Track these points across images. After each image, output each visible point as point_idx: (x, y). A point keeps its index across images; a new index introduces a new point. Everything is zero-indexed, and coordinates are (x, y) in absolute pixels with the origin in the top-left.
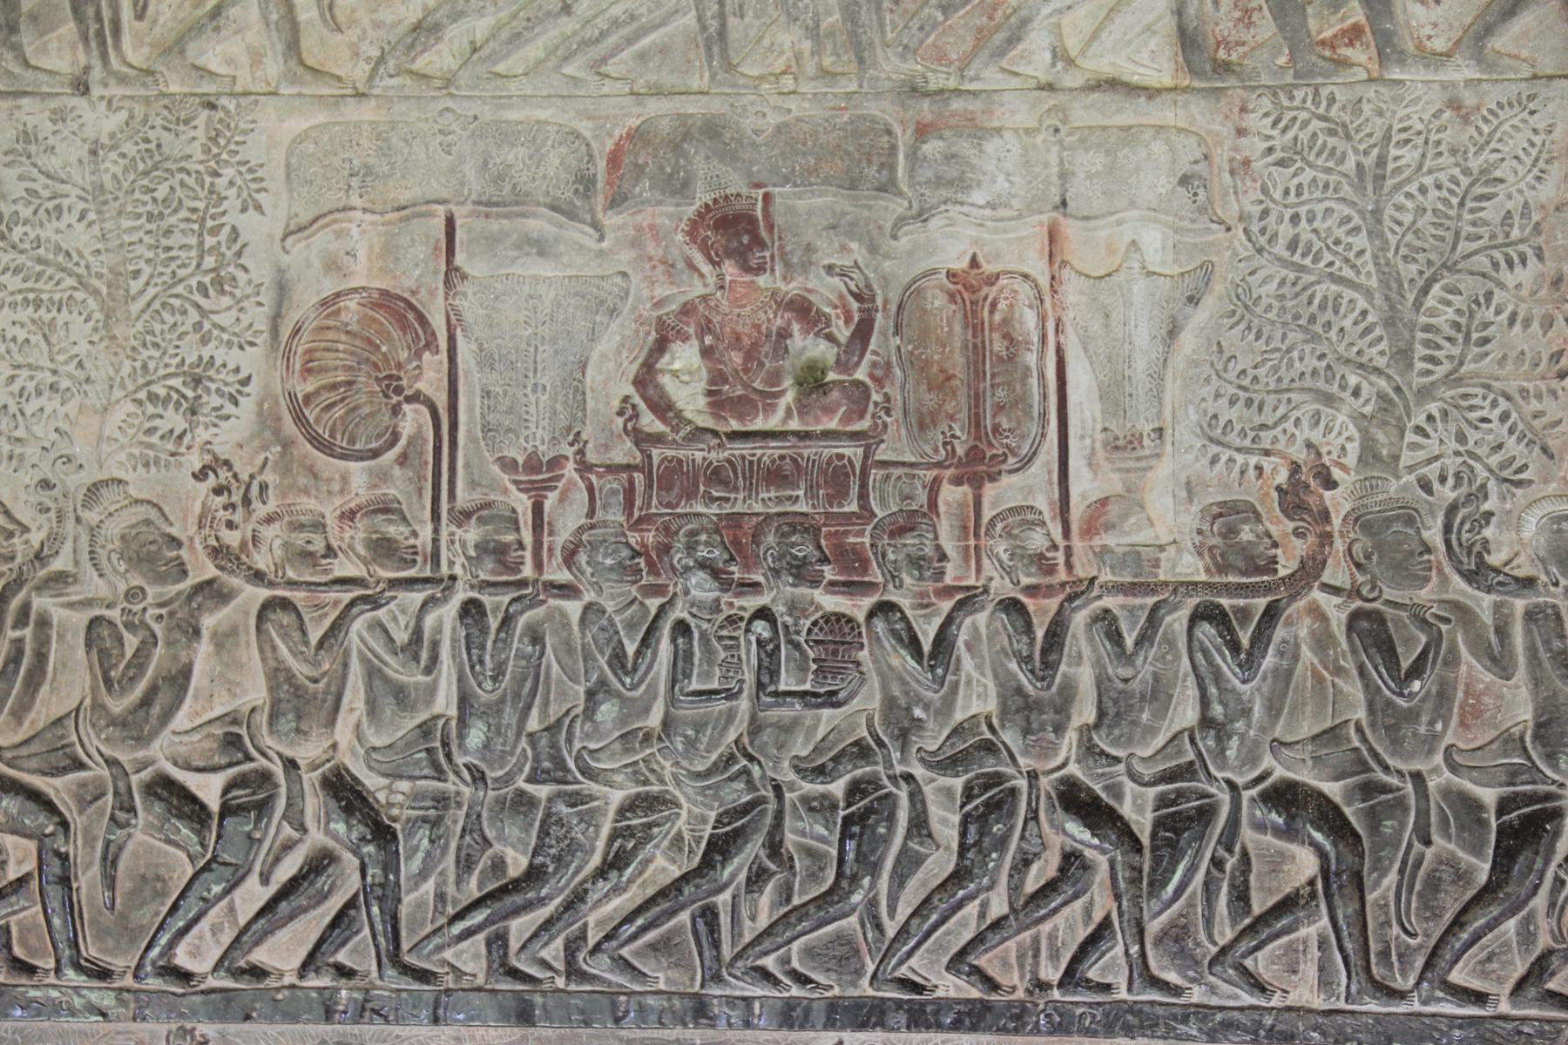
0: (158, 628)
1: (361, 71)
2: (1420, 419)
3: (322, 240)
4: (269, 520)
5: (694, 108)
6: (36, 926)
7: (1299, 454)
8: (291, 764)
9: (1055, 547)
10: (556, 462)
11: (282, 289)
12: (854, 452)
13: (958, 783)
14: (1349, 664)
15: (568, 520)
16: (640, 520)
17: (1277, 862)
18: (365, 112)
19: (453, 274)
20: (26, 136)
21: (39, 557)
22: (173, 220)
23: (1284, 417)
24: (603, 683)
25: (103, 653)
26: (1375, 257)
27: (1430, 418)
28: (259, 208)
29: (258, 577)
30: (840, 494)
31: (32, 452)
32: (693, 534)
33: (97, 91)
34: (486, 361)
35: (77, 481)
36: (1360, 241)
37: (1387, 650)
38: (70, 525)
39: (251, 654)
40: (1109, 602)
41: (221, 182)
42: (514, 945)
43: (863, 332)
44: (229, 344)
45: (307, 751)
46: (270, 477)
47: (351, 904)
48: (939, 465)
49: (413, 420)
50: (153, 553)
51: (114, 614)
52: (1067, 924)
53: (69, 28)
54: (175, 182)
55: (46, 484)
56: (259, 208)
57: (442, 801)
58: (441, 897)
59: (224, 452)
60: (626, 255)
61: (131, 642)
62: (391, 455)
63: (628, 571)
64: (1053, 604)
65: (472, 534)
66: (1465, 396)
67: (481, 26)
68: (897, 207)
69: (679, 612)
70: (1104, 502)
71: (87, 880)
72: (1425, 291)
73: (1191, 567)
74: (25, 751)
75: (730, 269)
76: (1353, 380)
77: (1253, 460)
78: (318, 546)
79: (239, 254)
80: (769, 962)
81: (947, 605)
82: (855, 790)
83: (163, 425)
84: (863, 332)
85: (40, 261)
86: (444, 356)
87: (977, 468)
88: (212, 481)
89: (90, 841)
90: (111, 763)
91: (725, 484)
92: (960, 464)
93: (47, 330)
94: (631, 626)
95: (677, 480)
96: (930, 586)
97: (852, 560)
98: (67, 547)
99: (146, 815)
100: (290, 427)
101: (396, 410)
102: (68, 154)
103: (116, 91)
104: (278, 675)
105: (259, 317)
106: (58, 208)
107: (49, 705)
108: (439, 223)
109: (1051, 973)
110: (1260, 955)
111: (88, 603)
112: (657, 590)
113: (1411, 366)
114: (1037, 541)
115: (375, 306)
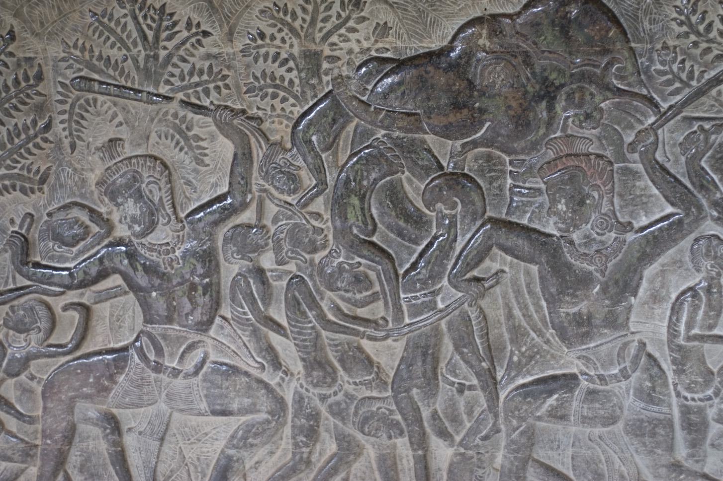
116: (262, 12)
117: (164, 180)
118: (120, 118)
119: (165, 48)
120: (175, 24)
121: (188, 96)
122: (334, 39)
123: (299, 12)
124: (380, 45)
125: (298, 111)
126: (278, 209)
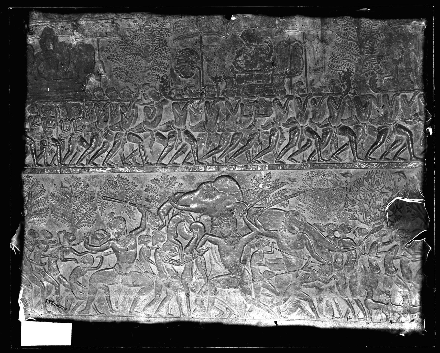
0: (156, 108)
2: (365, 64)
4: (173, 89)
7: (345, 70)
8: (179, 129)
9: (305, 88)
10: (221, 77)
13: (289, 129)
14: (354, 106)
16: (235, 86)
17: (343, 139)
22: (155, 39)
23: (343, 64)
26: (357, 36)
27: (367, 63)
28: (169, 36)
29: (172, 99)
32: (243, 88)
36: (355, 33)
40: (315, 97)
42: (217, 158)
44: (165, 59)
45: (182, 127)
48: (284, 75)
51: (149, 106)
52: (308, 152)
54: (155, 32)
56: (169, 36)
61: (152, 110)
62: (193, 77)
64: (305, 98)
66: (373, 60)
69: (242, 102)
70: (313, 80)
72: (366, 42)
76: (354, 57)
77: (338, 72)
79: (166, 44)
80: (258, 159)
81: (286, 99)
82: (272, 130)
85: (133, 47)
92: (288, 75)
93: (134, 58)
95: (241, 80)
96: (283, 95)
98: (140, 95)
106: (135, 38)
107: (139, 121)
109: (306, 159)
110: (340, 155)
111: (144, 104)
113: (364, 55)
114: (302, 87)
116: (151, 180)
117: (124, 223)
118: (114, 207)
119: (126, 189)
120: (129, 183)
121: (131, 201)
122: (169, 187)
123: (160, 180)
124: (180, 189)
125: (159, 206)
126: (153, 231)
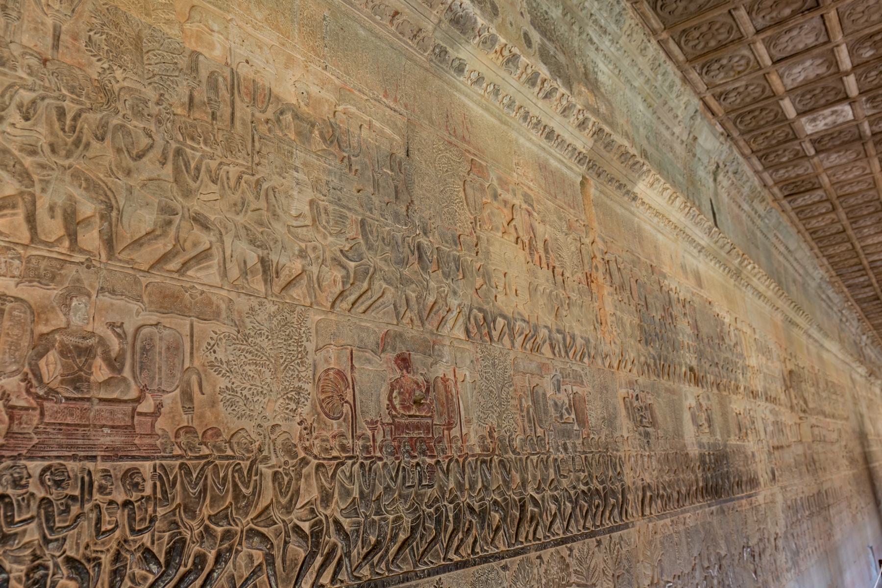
0: (292, 474)
1: (329, 305)
3: (324, 352)
4: (316, 438)
5: (396, 329)
6: (264, 581)
8: (326, 516)
10: (377, 422)
11: (315, 366)
12: (430, 421)
15: (379, 439)
18: (332, 317)
19: (352, 366)
20: (252, 309)
21: (260, 450)
24: (388, 485)
25: (280, 484)
29: (315, 457)
30: (428, 433)
31: (255, 414)
33: (270, 298)
34: (361, 393)
35: (267, 424)
37: (505, 467)
38: (267, 439)
39: (314, 482)
41: (302, 332)
43: (428, 390)
46: (315, 425)
47: (340, 559)
49: (346, 408)
50: (290, 450)
51: (281, 470)
53: (259, 276)
55: (260, 426)
57: (359, 523)
58: (359, 553)
59: (304, 416)
60: (385, 366)
61: (286, 479)
62: (342, 419)
63: (392, 454)
65: (360, 443)
67: (352, 298)
68: (431, 360)
71: (278, 562)
73: (478, 450)
74: (259, 520)
75: (405, 371)
78: (328, 447)
81: (447, 461)
82: (437, 509)
83: (290, 407)
84: (428, 390)
85: (257, 350)
86: (351, 390)
87: (449, 426)
88: (303, 426)
89: (279, 549)
90: (284, 521)
91: (409, 429)
94: (394, 469)
95: (398, 427)
97: (430, 449)
99: (293, 538)
100: (319, 409)
101: (342, 405)
102: (262, 317)
103: (274, 299)
104: (322, 488)
105: (310, 373)
108: (348, 351)
109: (469, 552)
112: (397, 458)
115: (337, 374)
